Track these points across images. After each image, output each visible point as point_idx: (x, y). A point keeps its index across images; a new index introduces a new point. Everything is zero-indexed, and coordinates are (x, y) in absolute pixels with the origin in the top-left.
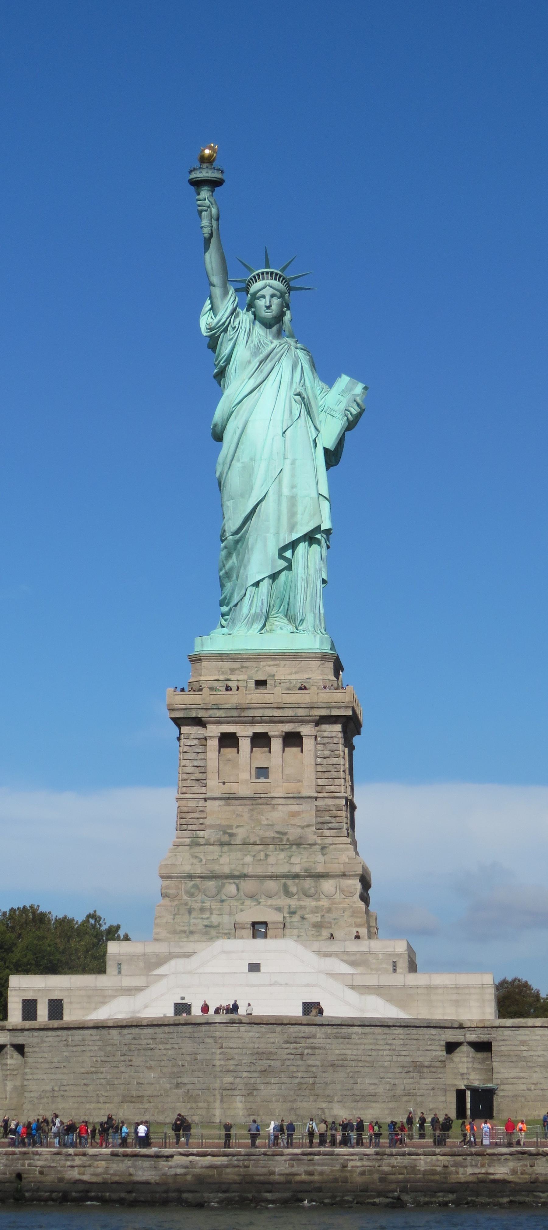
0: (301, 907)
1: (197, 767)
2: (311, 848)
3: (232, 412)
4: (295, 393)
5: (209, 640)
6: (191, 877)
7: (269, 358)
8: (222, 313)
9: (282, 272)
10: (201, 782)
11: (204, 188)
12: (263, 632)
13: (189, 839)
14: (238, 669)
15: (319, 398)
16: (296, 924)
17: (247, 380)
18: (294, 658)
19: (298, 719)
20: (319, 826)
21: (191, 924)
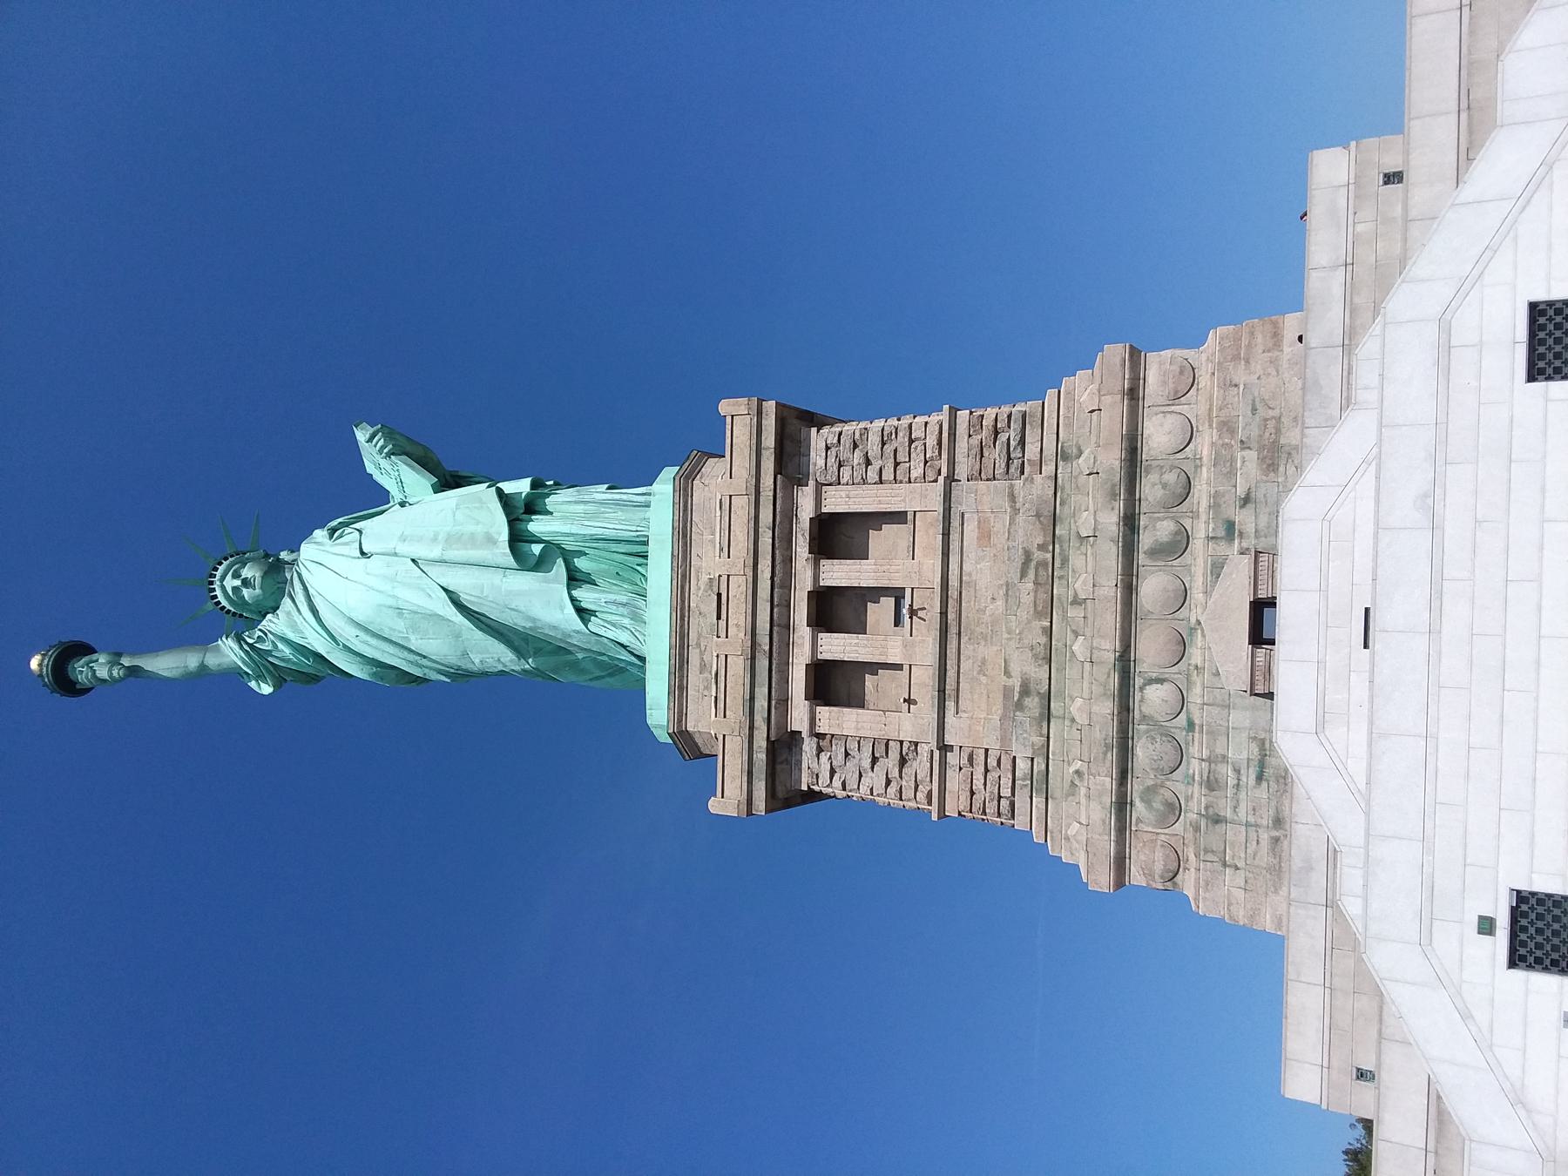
0: (1215, 506)
2: (1063, 489)
3: (344, 646)
6: (1122, 805)
10: (907, 754)
13: (1034, 798)
16: (1263, 520)
18: (685, 536)
20: (1012, 470)
21: (1251, 819)
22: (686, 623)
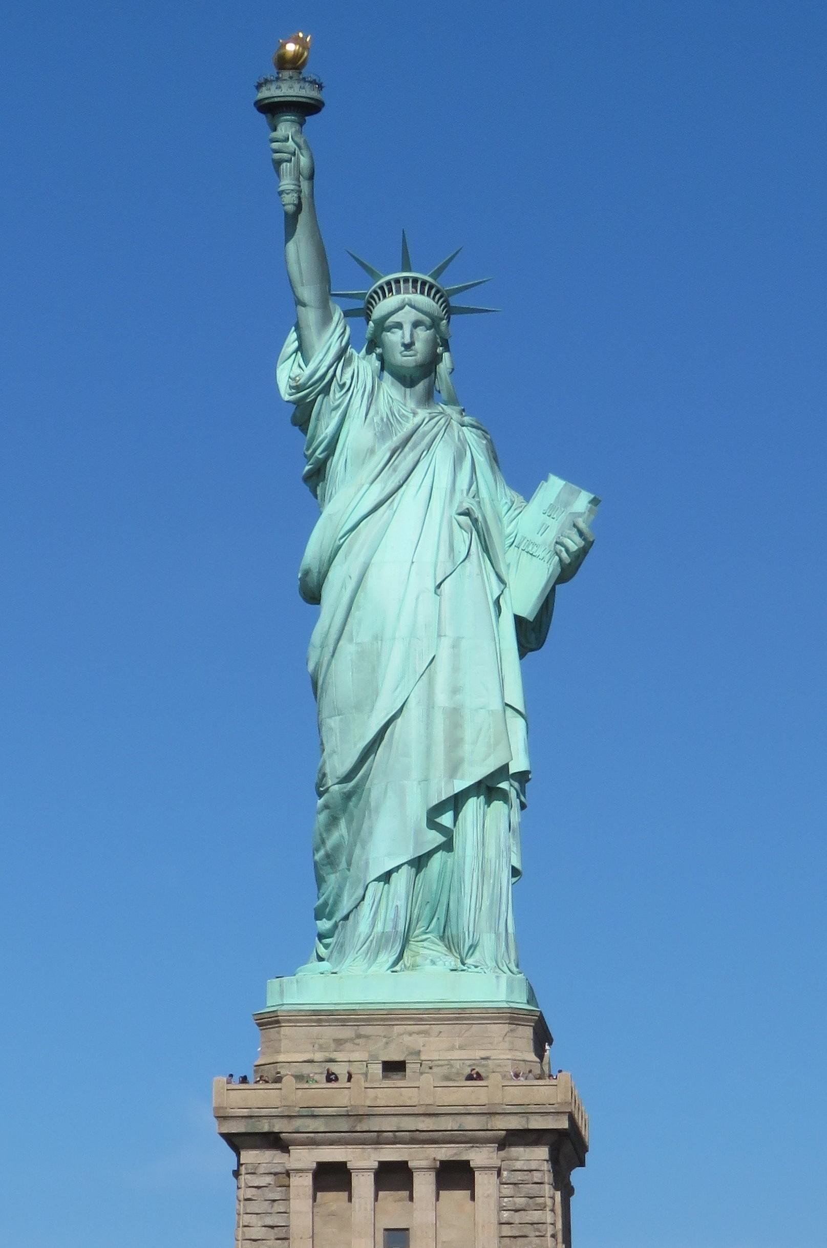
1: (272, 1227)
3: (340, 547)
4: (460, 511)
5: (295, 985)
7: (410, 444)
8: (320, 357)
9: (435, 279)
11: (285, 117)
12: (397, 968)
14: (351, 1040)
15: (505, 520)
17: (368, 485)
18: (457, 1019)
19: (465, 1135)
22: (378, 1023)
